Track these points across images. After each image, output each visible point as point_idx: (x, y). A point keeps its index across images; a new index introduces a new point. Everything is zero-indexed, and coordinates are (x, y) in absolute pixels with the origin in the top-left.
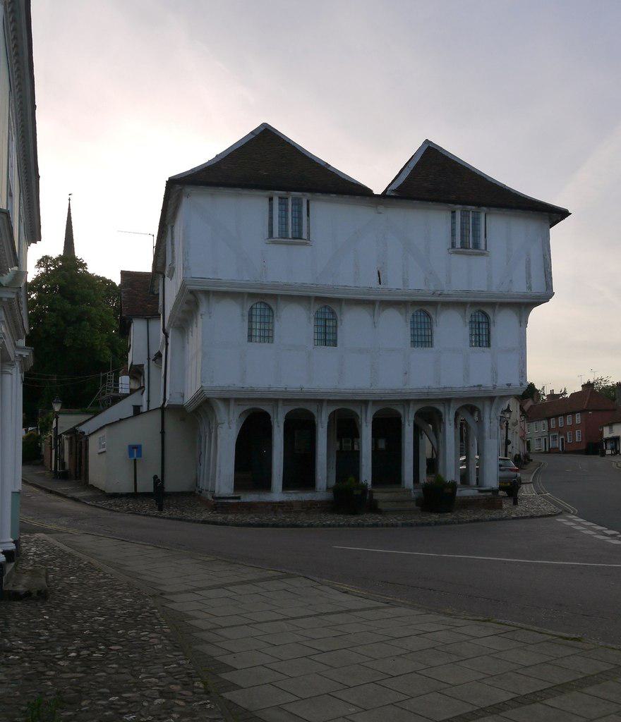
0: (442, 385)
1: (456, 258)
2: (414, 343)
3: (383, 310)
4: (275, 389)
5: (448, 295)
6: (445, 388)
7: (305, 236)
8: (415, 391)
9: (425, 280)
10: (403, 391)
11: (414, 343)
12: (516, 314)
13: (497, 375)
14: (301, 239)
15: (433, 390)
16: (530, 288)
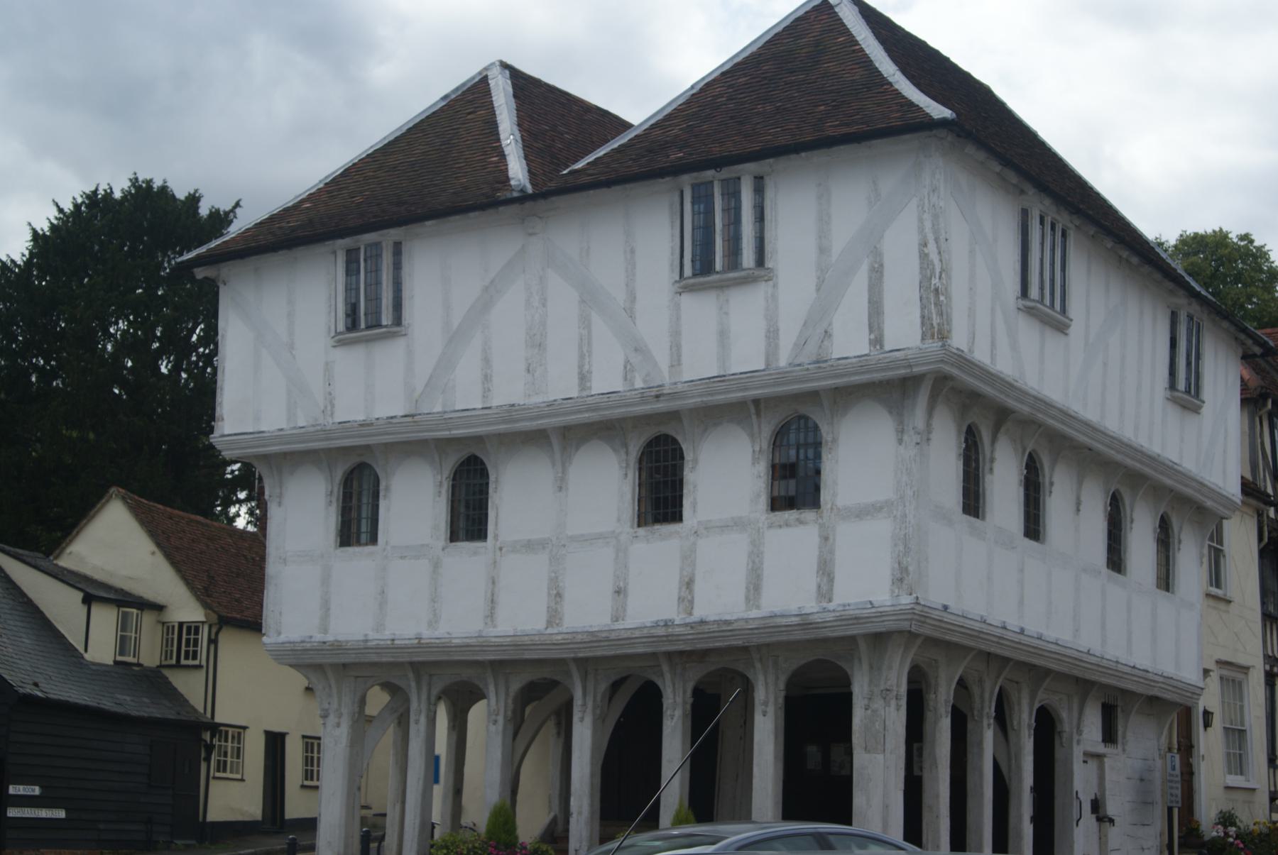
0: (698, 614)
1: (687, 300)
2: (779, 503)
3: (577, 449)
4: (374, 643)
5: (673, 396)
6: (702, 622)
7: (386, 319)
8: (637, 634)
9: (625, 367)
10: (613, 636)
11: (779, 503)
12: (890, 413)
13: (831, 580)
14: (379, 325)
15: (678, 630)
16: (877, 341)
